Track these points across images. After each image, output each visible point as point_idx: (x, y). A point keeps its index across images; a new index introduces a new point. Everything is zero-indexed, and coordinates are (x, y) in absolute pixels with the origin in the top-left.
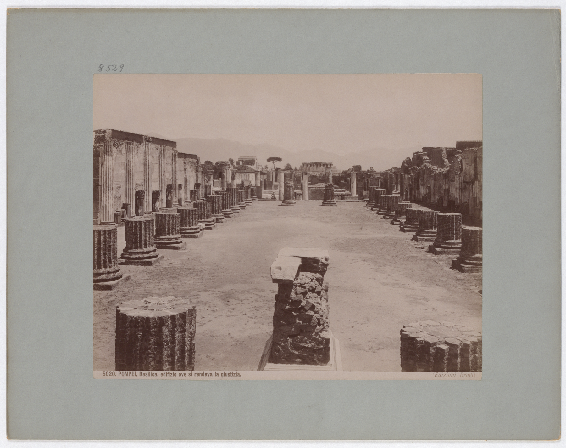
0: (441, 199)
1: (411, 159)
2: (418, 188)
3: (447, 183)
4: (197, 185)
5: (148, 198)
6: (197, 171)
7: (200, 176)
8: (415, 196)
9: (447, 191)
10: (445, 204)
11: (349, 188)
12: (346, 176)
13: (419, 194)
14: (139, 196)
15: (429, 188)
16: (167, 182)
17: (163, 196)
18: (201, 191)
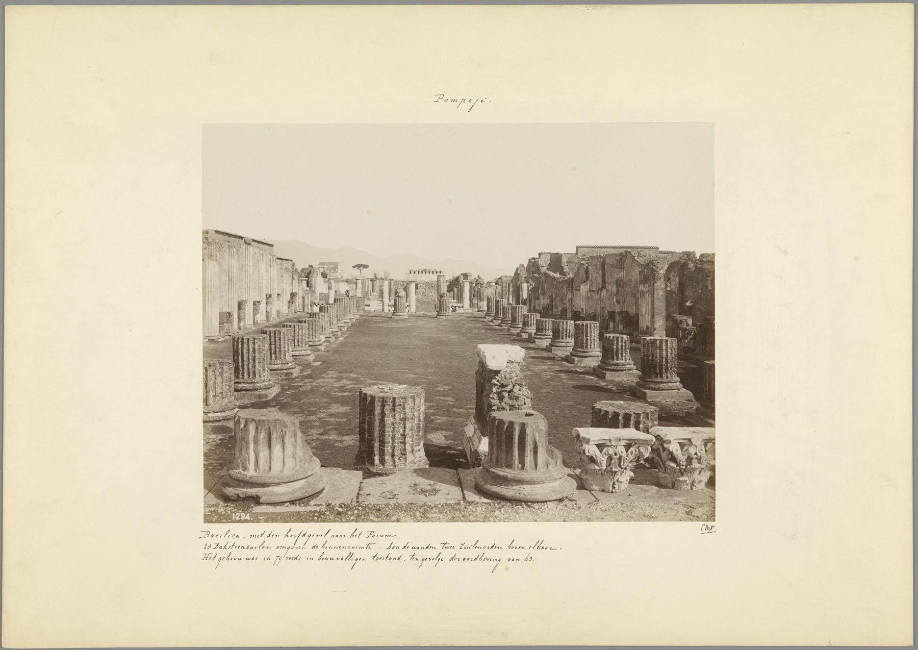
0: (564, 311)
1: (526, 265)
2: (539, 299)
3: (571, 292)
4: (293, 295)
5: (249, 308)
6: (293, 278)
7: (297, 285)
8: (534, 307)
9: (572, 300)
10: (569, 314)
11: (460, 298)
12: (455, 285)
13: (539, 304)
14: (240, 306)
15: (551, 297)
16: (266, 291)
17: (263, 307)
18: (298, 300)
